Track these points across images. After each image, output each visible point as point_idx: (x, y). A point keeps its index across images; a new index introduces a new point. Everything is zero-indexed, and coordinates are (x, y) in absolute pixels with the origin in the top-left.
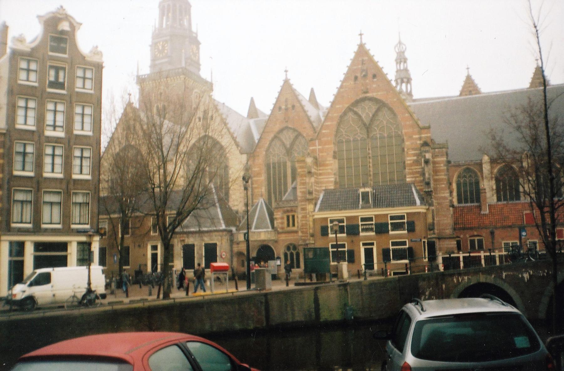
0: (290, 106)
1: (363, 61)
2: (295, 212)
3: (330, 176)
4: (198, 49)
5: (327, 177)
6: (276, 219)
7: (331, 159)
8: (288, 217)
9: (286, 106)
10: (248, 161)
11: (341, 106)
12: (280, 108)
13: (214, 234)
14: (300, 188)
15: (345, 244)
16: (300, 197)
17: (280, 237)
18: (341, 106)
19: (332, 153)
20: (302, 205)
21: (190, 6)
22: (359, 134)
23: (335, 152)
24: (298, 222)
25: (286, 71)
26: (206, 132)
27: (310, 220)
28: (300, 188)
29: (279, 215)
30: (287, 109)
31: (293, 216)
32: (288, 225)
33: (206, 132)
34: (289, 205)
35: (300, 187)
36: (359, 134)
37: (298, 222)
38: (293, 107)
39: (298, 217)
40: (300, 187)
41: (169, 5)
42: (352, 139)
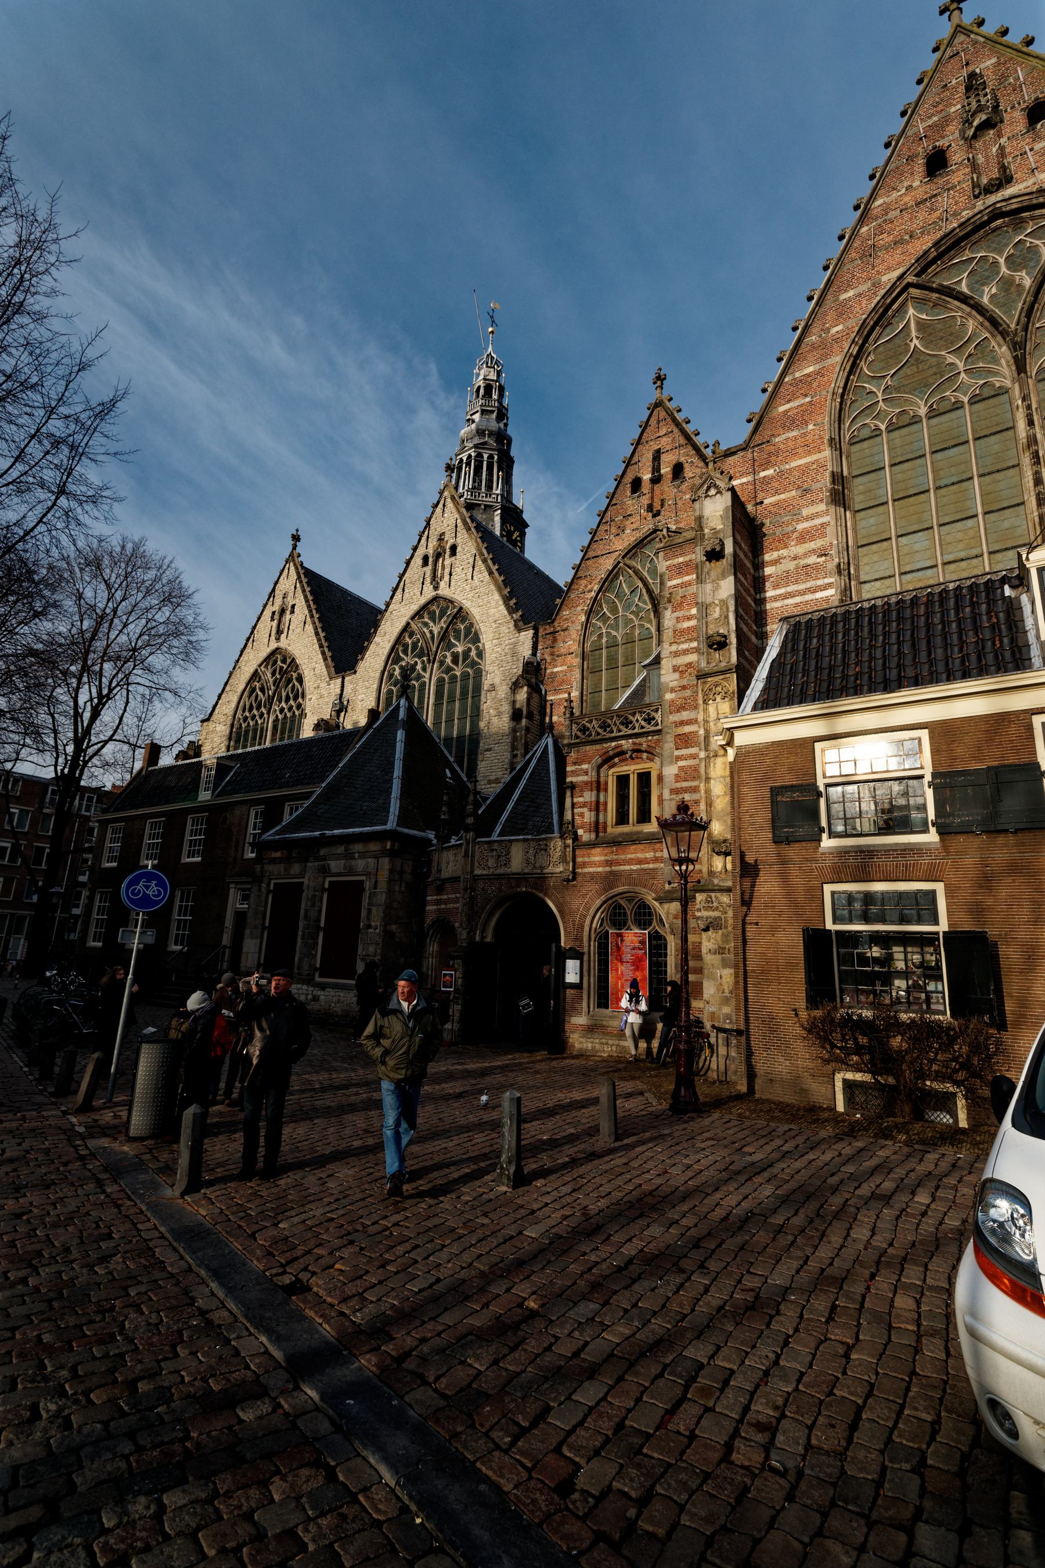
0: (666, 470)
1: (972, 76)
2: (651, 754)
3: (820, 582)
4: (523, 535)
5: (802, 587)
6: (573, 787)
7: (822, 507)
8: (623, 781)
9: (656, 469)
10: (535, 648)
11: (864, 287)
12: (636, 484)
13: (358, 847)
14: (676, 654)
15: (933, 893)
16: (672, 690)
17: (584, 865)
18: (864, 287)
19: (825, 480)
20: (682, 723)
21: (513, 462)
22: (963, 375)
23: (837, 478)
24: (661, 801)
25: (660, 379)
26: (436, 588)
27: (712, 774)
28: (676, 654)
29: (586, 773)
30: (656, 480)
31: (644, 778)
32: (622, 818)
33: (436, 588)
34: (625, 731)
35: (674, 648)
36: (963, 375)
37: (661, 801)
38: (678, 470)
39: (660, 778)
40: (674, 648)
41: (470, 456)
42: (923, 411)
